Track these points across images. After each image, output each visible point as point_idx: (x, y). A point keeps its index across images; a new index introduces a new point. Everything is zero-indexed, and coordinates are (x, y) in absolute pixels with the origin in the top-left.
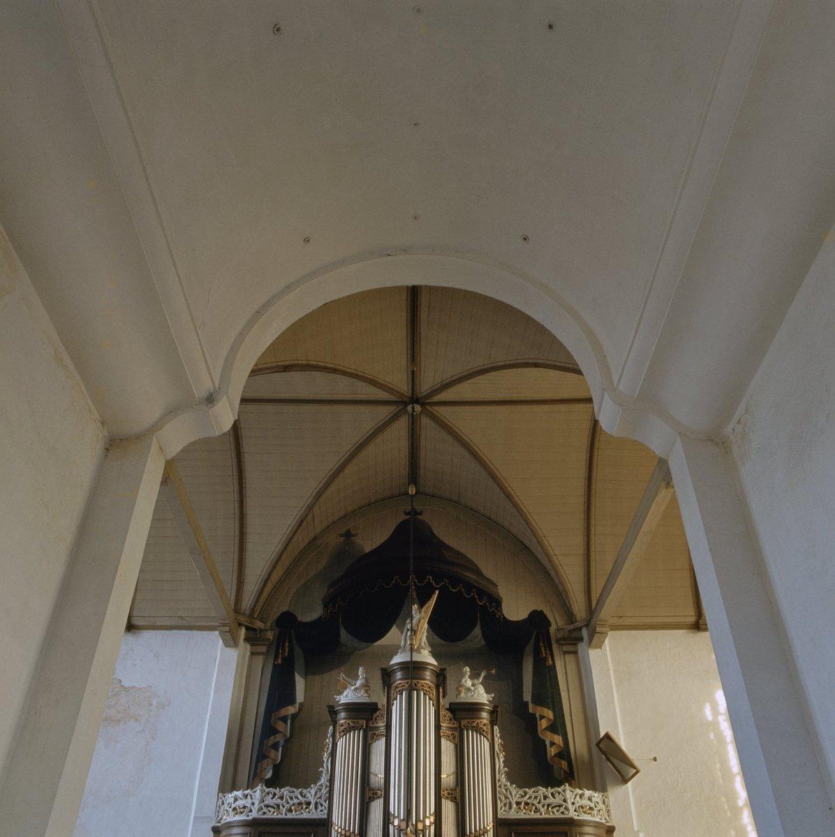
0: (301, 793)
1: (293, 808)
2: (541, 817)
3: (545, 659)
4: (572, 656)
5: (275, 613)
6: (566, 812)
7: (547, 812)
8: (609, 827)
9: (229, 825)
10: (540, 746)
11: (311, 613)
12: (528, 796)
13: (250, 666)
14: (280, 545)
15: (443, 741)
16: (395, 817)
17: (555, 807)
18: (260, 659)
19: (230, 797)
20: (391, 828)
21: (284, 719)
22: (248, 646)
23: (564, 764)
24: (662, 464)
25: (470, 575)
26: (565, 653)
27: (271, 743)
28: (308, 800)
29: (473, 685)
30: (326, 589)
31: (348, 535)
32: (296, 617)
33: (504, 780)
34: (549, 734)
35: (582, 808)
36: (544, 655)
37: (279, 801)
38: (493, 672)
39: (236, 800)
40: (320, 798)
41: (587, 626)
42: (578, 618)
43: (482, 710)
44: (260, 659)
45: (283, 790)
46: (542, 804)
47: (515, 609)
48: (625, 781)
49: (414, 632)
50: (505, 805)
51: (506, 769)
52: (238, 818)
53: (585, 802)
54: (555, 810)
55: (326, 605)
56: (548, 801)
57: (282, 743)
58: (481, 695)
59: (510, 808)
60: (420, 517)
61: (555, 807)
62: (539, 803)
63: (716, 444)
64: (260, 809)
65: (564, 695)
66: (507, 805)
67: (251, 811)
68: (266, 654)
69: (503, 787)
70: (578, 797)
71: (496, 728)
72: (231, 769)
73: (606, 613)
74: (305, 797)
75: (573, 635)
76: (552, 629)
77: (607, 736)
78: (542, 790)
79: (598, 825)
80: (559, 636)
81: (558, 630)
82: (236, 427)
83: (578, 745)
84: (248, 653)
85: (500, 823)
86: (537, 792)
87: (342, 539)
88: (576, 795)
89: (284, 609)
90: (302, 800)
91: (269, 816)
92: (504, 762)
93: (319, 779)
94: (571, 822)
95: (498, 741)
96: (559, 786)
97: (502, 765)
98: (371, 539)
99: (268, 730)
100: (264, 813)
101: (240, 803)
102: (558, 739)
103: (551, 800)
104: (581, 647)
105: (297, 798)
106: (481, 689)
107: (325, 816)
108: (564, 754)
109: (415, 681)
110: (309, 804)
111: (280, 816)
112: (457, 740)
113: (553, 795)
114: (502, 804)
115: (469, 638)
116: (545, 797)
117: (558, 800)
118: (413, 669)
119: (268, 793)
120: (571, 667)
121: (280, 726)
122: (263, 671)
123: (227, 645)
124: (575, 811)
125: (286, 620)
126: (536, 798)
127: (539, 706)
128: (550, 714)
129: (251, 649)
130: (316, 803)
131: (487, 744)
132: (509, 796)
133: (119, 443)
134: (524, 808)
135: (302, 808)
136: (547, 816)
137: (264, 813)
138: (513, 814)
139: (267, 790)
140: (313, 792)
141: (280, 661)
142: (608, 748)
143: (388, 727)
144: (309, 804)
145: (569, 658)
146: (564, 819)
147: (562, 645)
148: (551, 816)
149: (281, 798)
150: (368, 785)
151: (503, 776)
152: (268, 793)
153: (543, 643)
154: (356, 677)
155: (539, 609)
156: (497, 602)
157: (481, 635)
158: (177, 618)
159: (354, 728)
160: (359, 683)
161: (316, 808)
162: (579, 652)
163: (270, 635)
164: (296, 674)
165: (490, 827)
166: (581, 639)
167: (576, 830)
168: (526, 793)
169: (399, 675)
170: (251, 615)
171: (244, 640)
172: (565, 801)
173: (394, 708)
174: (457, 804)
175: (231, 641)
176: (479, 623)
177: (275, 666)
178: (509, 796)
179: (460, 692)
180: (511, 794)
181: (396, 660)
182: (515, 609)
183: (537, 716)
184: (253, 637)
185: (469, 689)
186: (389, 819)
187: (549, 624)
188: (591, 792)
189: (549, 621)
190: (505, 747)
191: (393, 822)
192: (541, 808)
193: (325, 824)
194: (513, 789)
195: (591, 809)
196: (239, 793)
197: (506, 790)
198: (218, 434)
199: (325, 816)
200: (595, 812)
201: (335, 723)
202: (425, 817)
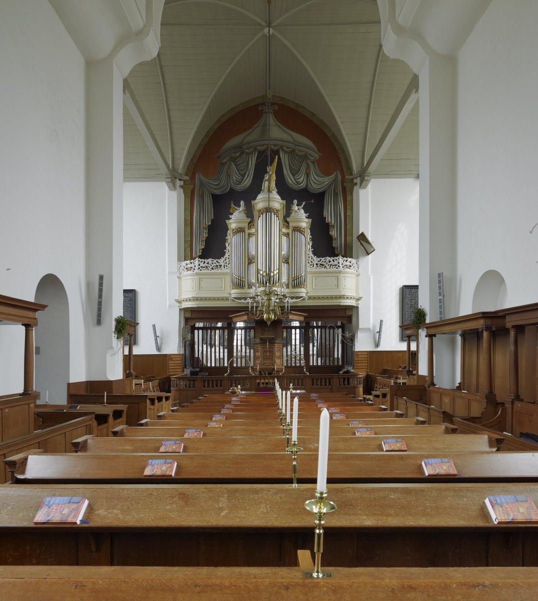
0: (217, 261)
16: (260, 271)
19: (184, 263)
20: (259, 275)
24: (416, 78)
28: (220, 264)
29: (298, 209)
40: (226, 263)
41: (360, 176)
48: (368, 254)
50: (311, 265)
53: (348, 263)
54: (333, 267)
63: (448, 62)
67: (194, 269)
73: (372, 168)
74: (219, 263)
77: (363, 234)
78: (328, 258)
82: (159, 54)
90: (218, 264)
93: (225, 255)
97: (311, 248)
101: (189, 266)
103: (332, 263)
104: (355, 188)
110: (221, 266)
113: (333, 260)
116: (330, 262)
117: (336, 263)
119: (201, 262)
123: (171, 189)
132: (313, 261)
137: (201, 270)
139: (201, 260)
142: (362, 238)
144: (221, 266)
149: (208, 263)
152: (201, 262)
167: (341, 275)
168: (321, 260)
172: (339, 263)
175: (173, 187)
194: (315, 258)
195: (350, 266)
196: (188, 262)
198: (149, 59)
200: (352, 268)
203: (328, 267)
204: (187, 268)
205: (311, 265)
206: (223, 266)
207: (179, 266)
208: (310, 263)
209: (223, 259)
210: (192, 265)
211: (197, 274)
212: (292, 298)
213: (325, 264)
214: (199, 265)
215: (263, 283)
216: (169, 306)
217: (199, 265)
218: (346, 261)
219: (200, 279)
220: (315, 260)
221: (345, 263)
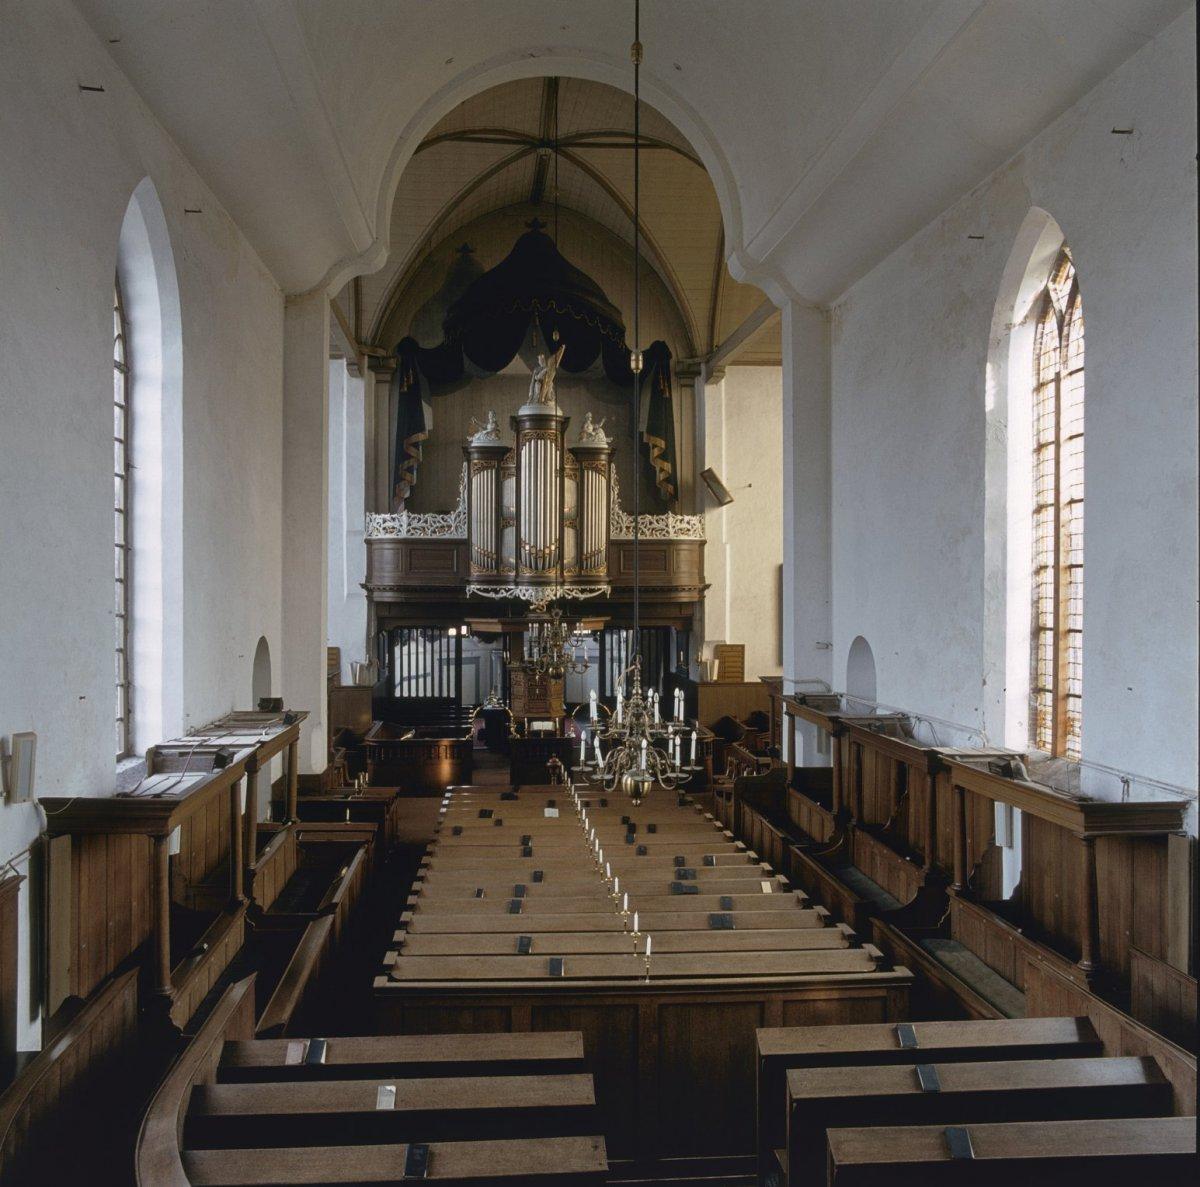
0: (443, 519)
4: (688, 390)
7: (652, 534)
8: (701, 541)
9: (381, 541)
10: (649, 472)
11: (432, 340)
13: (377, 397)
14: (398, 274)
15: (566, 480)
18: (386, 387)
19: (379, 518)
21: (416, 445)
22: (373, 374)
23: (670, 488)
25: (594, 300)
26: (682, 386)
27: (405, 467)
29: (594, 430)
30: (446, 314)
31: (466, 250)
32: (417, 344)
34: (659, 461)
38: (613, 418)
39: (385, 521)
42: (699, 353)
43: (601, 453)
44: (386, 387)
49: (541, 382)
52: (388, 536)
53: (684, 525)
56: (653, 526)
57: (416, 466)
58: (602, 441)
59: (621, 531)
60: (542, 230)
64: (409, 531)
65: (677, 425)
67: (400, 531)
68: (392, 382)
71: (613, 466)
72: (372, 491)
75: (692, 369)
79: (692, 542)
80: (678, 370)
83: (684, 472)
84: (374, 382)
85: (610, 543)
87: (459, 255)
89: (405, 335)
90: (445, 524)
93: (457, 507)
94: (671, 543)
95: (613, 476)
96: (663, 514)
97: (616, 496)
98: (490, 258)
99: (402, 455)
101: (389, 524)
102: (667, 466)
103: (655, 525)
105: (439, 522)
106: (602, 434)
107: (466, 537)
108: (672, 479)
109: (543, 431)
110: (450, 527)
111: (426, 537)
112: (578, 479)
113: (657, 521)
115: (590, 368)
116: (651, 523)
117: (661, 525)
118: (540, 421)
119: (414, 519)
120: (687, 402)
121: (413, 451)
123: (352, 374)
125: (408, 347)
127: (653, 435)
128: (662, 444)
130: (456, 527)
131: (604, 481)
133: (293, 301)
136: (651, 538)
138: (623, 536)
140: (453, 517)
141: (406, 389)
142: (710, 478)
143: (518, 468)
144: (450, 527)
145: (687, 392)
146: (665, 540)
148: (655, 537)
149: (426, 522)
150: (502, 515)
152: (414, 519)
154: (486, 421)
155: (661, 340)
159: (487, 468)
160: (490, 427)
162: (696, 386)
163: (393, 363)
164: (424, 403)
165: (603, 548)
169: (527, 424)
170: (373, 344)
171: (369, 367)
172: (667, 526)
173: (523, 452)
174: (577, 531)
175: (355, 369)
176: (601, 356)
177: (401, 394)
179: (581, 438)
181: (525, 411)
183: (651, 445)
184: (377, 365)
185: (591, 435)
186: (520, 544)
187: (669, 356)
188: (690, 517)
189: (670, 353)
190: (619, 482)
191: (524, 548)
193: (466, 543)
194: (625, 517)
195: (689, 530)
196: (387, 516)
199: (466, 537)
200: (691, 533)
201: (469, 461)
202: (551, 544)
203: (648, 533)
204: (384, 529)
207: (368, 519)
210: (396, 524)
211: (404, 541)
212: (583, 591)
215: (531, 567)
216: (348, 595)
217: (409, 525)
218: (681, 521)
220: (624, 519)
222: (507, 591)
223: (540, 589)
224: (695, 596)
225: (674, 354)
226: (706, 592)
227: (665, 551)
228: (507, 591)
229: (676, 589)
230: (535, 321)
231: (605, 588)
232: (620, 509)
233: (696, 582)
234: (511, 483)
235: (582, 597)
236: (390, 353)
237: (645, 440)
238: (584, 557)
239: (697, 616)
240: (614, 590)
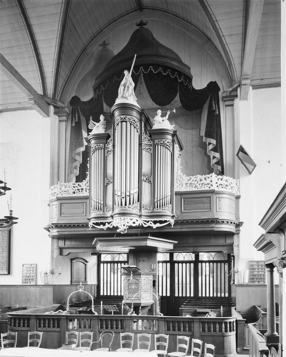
0: (79, 185)
1: (75, 192)
2: (198, 190)
3: (215, 111)
5: (69, 99)
6: (211, 187)
11: (87, 97)
12: (191, 180)
17: (206, 184)
20: (116, 197)
22: (57, 117)
26: (227, 106)
33: (180, 172)
35: (221, 185)
36: (214, 109)
37: (68, 189)
44: (64, 124)
45: (69, 184)
46: (199, 184)
47: (199, 83)
50: (180, 185)
51: (181, 167)
55: (95, 91)
56: (202, 182)
59: (182, 186)
61: (206, 184)
62: (197, 183)
66: (181, 185)
68: (66, 121)
69: (179, 176)
70: (220, 179)
74: (80, 186)
76: (220, 94)
78: (199, 177)
80: (224, 95)
81: (224, 92)
86: (197, 178)
88: (219, 179)
90: (79, 187)
91: (64, 196)
92: (180, 163)
94: (213, 192)
97: (179, 165)
100: (62, 194)
104: (237, 101)
110: (82, 189)
113: (205, 179)
114: (178, 185)
115: (172, 103)
117: (208, 181)
120: (229, 114)
122: (66, 129)
123: (44, 117)
124: (217, 186)
125: (75, 101)
126: (196, 180)
129: (59, 119)
130: (86, 189)
132: (182, 180)
134: (189, 186)
135: (79, 191)
137: (62, 194)
138: (183, 189)
144: (82, 189)
147: (225, 101)
151: (179, 171)
153: (215, 101)
156: (189, 79)
157: (179, 101)
158: (17, 104)
161: (86, 191)
162: (234, 105)
166: (237, 96)
167: (215, 196)
168: (191, 179)
172: (211, 181)
176: (178, 95)
178: (182, 180)
180: (183, 180)
182: (199, 83)
187: (219, 89)
192: (198, 186)
194: (184, 177)
197: (180, 177)
199: (88, 195)
200: (229, 187)
203: (199, 186)
205: (180, 185)
206: (84, 190)
208: (179, 183)
209: (84, 182)
211: (58, 199)
212: (155, 222)
213: (195, 183)
214: (61, 189)
218: (221, 179)
219: (61, 204)
221: (220, 182)
222: (109, 223)
223: (123, 218)
224: (230, 228)
225: (221, 88)
226: (241, 228)
227: (210, 197)
228: (109, 223)
229: (216, 221)
230: (141, 79)
231: (172, 221)
232: (182, 172)
233: (232, 218)
234: (110, 157)
235: (155, 226)
236: (66, 105)
237: (204, 140)
238: (156, 200)
239: (235, 244)
240: (176, 223)
